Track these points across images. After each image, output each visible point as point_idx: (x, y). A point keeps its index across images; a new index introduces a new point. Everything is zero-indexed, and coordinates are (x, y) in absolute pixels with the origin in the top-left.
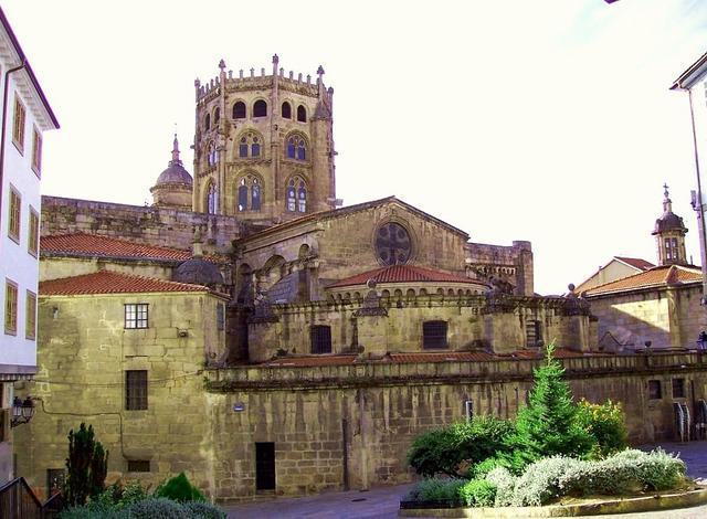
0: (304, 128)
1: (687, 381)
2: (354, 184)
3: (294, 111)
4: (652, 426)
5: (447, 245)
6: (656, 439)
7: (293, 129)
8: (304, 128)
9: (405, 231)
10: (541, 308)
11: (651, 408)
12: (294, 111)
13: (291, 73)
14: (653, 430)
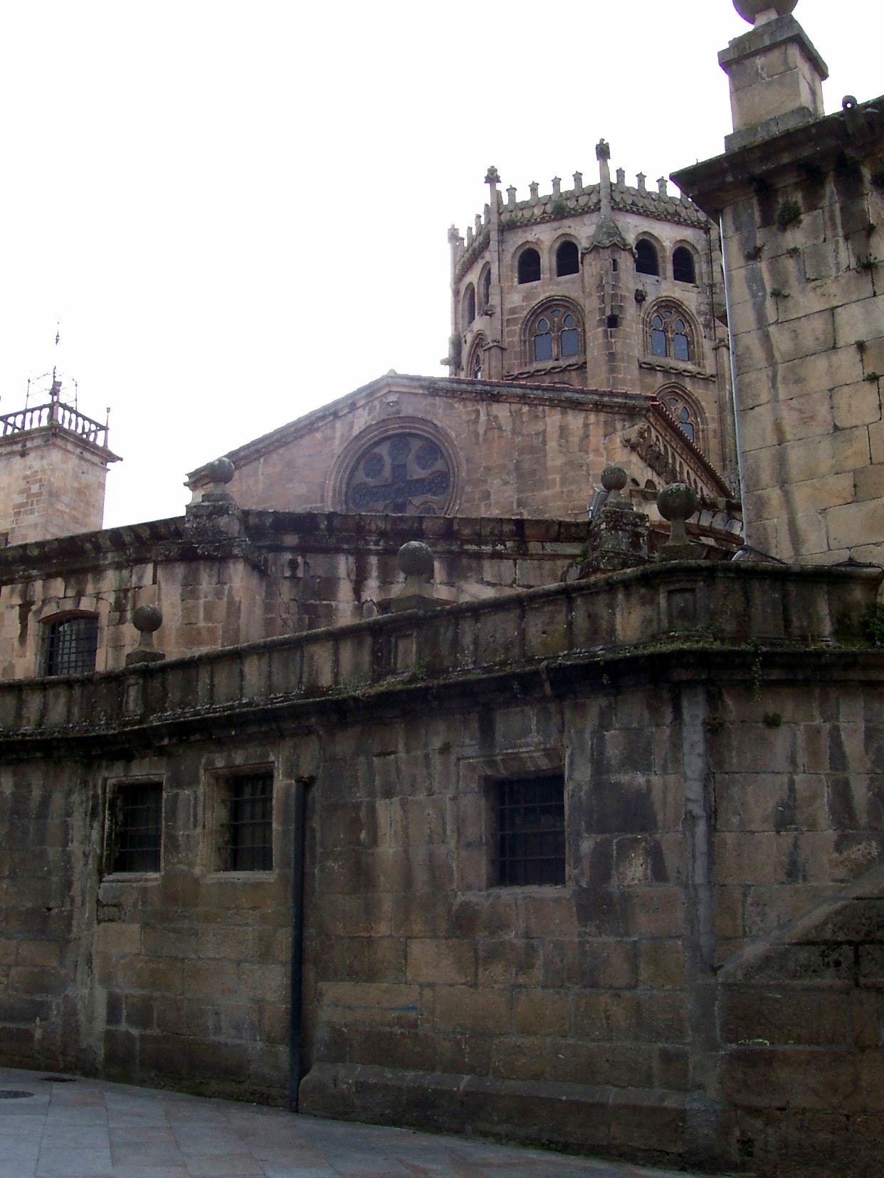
0: (565, 286)
1: (281, 783)
2: (444, 372)
3: (548, 261)
4: (101, 995)
5: (564, 449)
6: (109, 1058)
7: (542, 297)
8: (565, 286)
9: (433, 448)
10: (98, 571)
11: (109, 911)
12: (548, 261)
13: (641, 177)
14: (101, 1011)
